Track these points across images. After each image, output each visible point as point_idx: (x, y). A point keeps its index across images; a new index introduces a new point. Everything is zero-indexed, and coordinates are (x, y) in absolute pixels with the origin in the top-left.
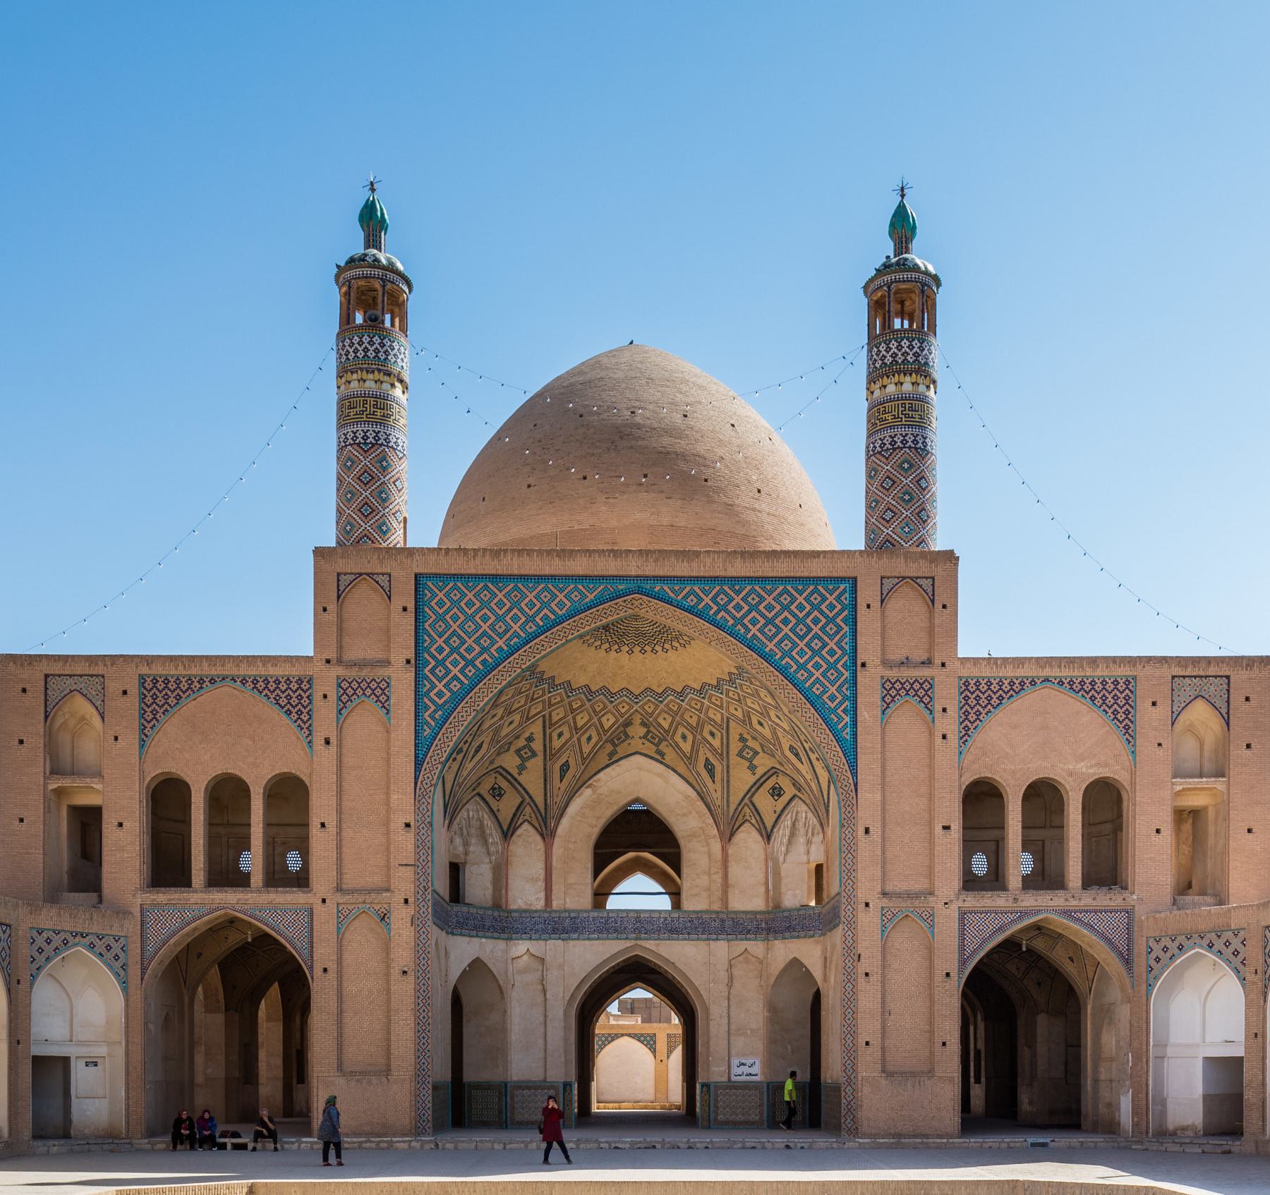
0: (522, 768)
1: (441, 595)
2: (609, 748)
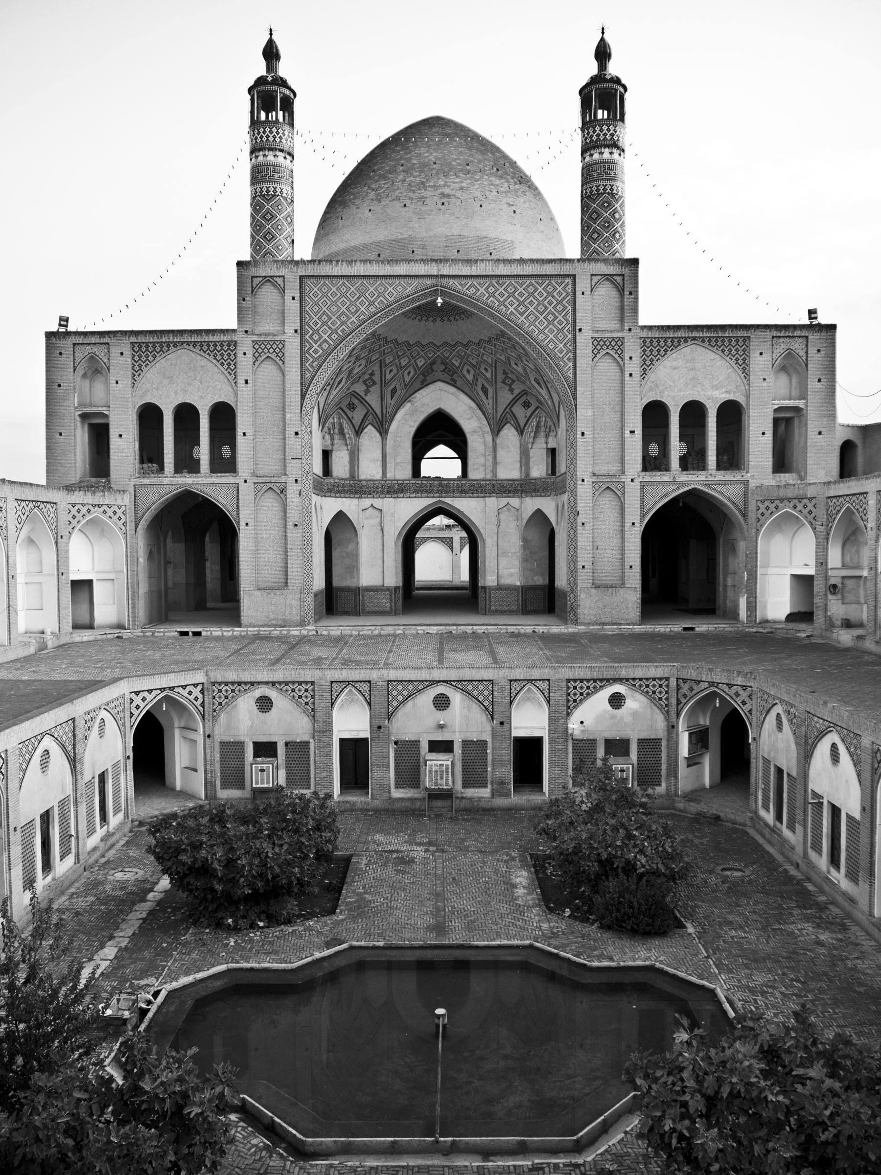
0: (367, 392)
1: (316, 289)
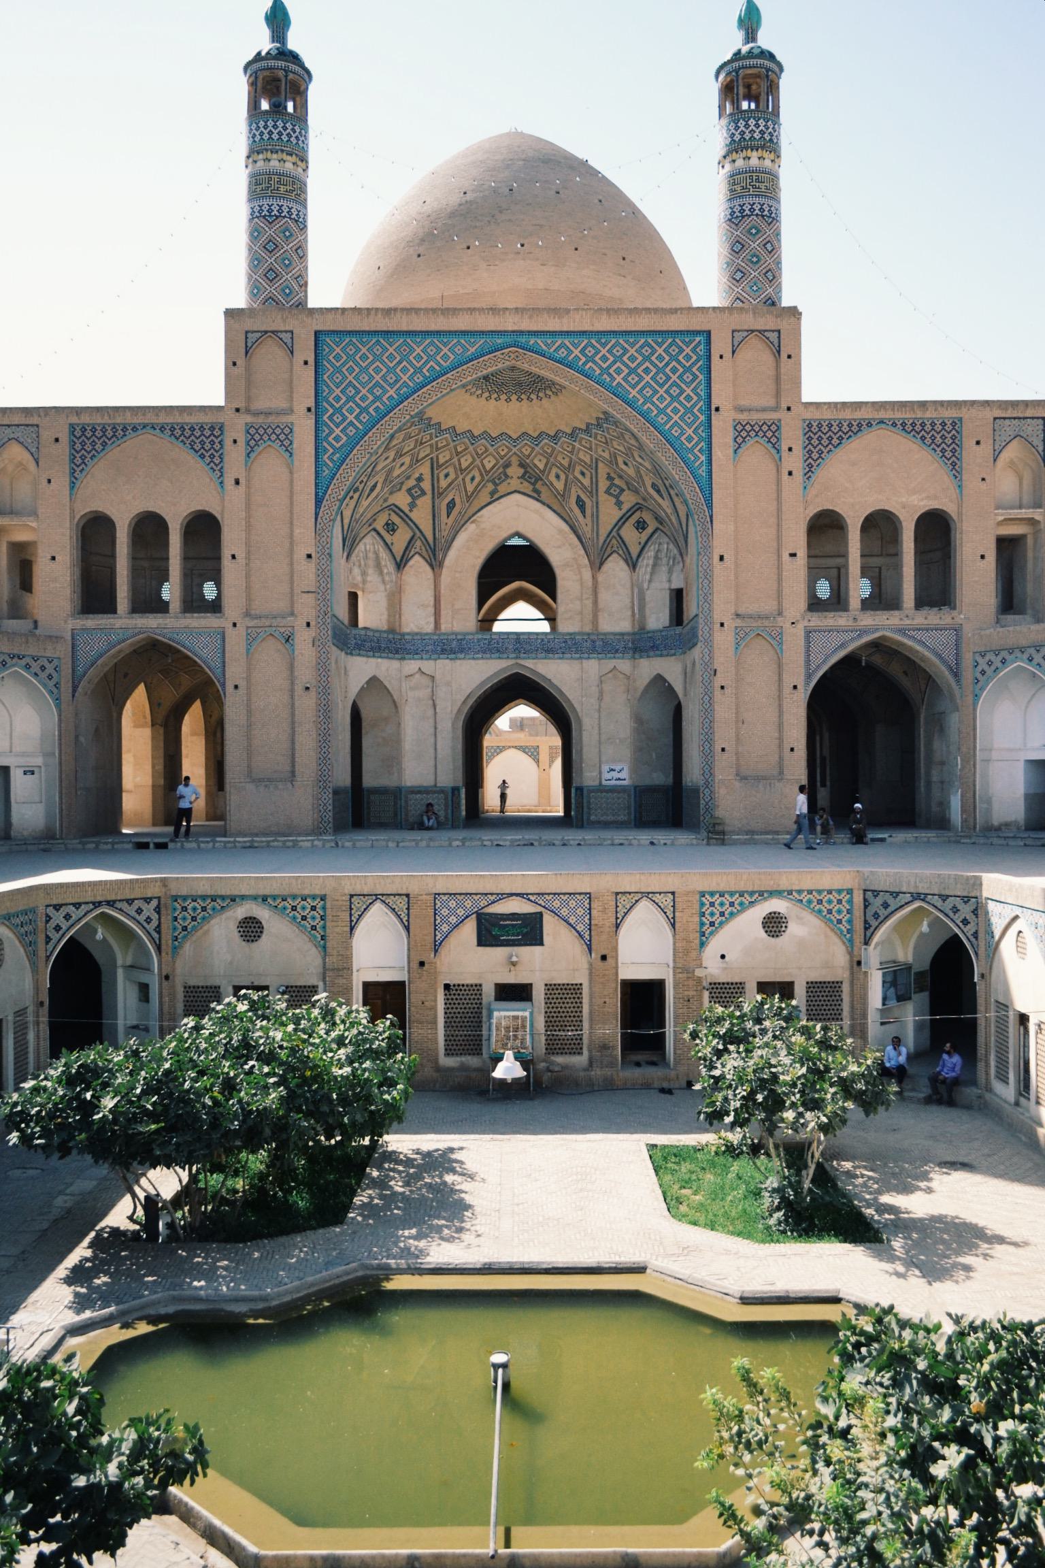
0: (412, 505)
2: (490, 487)
